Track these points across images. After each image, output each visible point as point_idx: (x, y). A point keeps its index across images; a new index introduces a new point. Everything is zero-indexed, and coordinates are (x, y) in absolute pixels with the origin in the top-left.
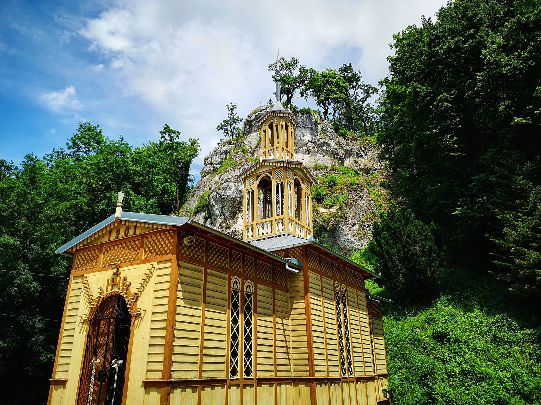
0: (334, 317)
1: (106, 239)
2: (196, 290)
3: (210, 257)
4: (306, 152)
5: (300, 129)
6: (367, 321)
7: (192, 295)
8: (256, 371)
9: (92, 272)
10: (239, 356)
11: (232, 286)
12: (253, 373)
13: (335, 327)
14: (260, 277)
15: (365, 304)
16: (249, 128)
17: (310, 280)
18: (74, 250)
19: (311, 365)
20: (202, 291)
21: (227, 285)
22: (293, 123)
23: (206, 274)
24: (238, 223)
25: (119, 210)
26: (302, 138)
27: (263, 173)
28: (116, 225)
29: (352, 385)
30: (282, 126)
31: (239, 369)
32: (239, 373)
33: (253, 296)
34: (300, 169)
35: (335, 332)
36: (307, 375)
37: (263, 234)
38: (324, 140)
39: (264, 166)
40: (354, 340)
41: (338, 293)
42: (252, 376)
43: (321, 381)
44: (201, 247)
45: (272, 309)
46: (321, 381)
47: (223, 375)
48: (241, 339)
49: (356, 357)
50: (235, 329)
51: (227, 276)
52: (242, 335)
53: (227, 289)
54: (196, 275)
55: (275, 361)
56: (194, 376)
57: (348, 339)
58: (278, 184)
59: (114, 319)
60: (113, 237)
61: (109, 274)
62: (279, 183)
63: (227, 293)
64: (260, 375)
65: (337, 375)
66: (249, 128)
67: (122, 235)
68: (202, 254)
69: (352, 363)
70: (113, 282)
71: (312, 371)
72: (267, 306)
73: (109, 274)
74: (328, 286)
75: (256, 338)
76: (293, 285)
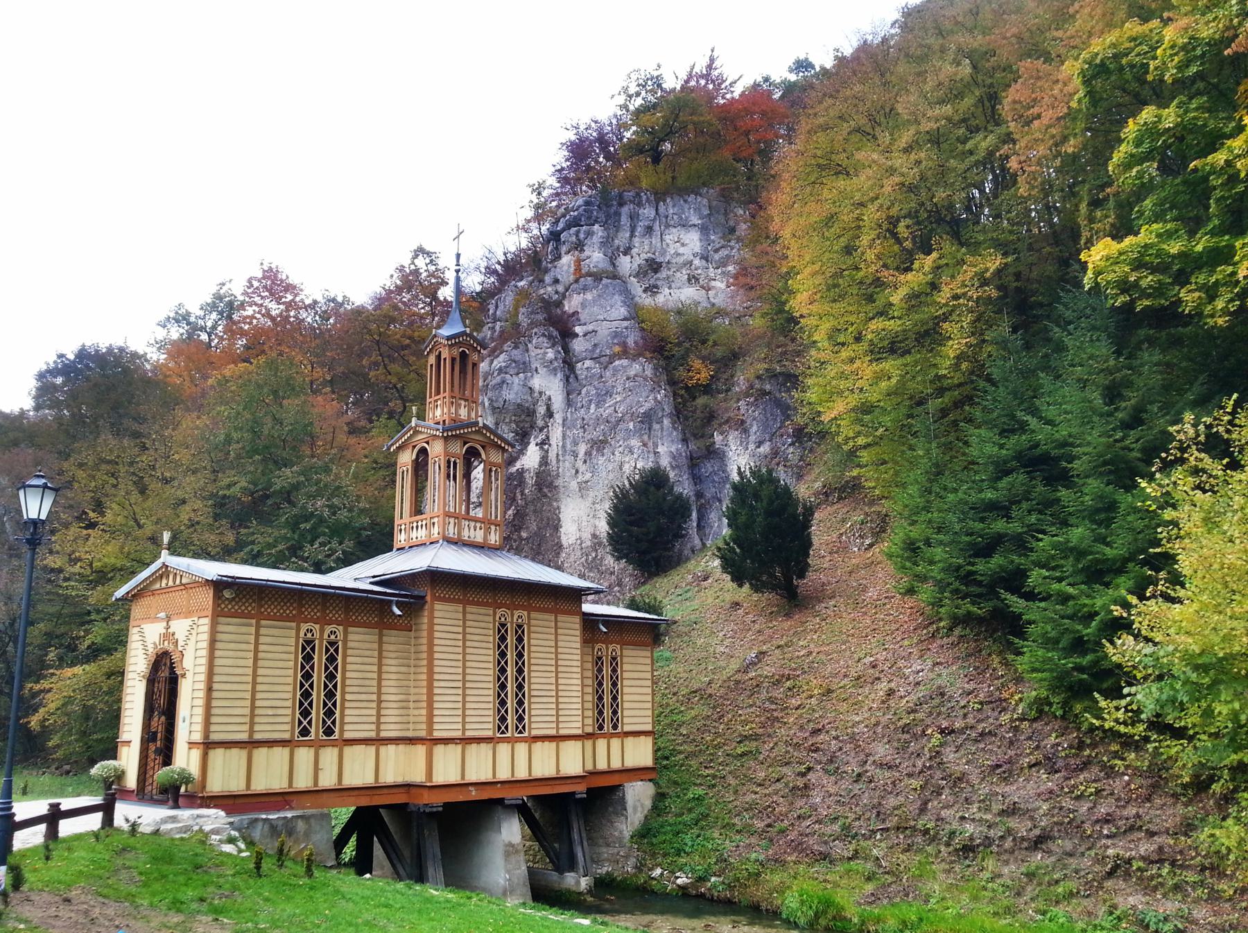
1: (157, 586)
2: (243, 646)
4: (689, 280)
5: (674, 230)
11: (302, 634)
16: (557, 248)
17: (437, 614)
20: (252, 647)
24: (529, 453)
25: (164, 553)
26: (681, 250)
30: (453, 360)
31: (313, 730)
34: (478, 432)
36: (423, 734)
38: (726, 252)
42: (336, 736)
47: (287, 736)
48: (318, 695)
51: (294, 624)
54: (244, 629)
59: (164, 678)
61: (159, 628)
64: (347, 735)
66: (557, 248)
67: (171, 583)
70: (168, 636)
71: (430, 730)
73: (159, 628)
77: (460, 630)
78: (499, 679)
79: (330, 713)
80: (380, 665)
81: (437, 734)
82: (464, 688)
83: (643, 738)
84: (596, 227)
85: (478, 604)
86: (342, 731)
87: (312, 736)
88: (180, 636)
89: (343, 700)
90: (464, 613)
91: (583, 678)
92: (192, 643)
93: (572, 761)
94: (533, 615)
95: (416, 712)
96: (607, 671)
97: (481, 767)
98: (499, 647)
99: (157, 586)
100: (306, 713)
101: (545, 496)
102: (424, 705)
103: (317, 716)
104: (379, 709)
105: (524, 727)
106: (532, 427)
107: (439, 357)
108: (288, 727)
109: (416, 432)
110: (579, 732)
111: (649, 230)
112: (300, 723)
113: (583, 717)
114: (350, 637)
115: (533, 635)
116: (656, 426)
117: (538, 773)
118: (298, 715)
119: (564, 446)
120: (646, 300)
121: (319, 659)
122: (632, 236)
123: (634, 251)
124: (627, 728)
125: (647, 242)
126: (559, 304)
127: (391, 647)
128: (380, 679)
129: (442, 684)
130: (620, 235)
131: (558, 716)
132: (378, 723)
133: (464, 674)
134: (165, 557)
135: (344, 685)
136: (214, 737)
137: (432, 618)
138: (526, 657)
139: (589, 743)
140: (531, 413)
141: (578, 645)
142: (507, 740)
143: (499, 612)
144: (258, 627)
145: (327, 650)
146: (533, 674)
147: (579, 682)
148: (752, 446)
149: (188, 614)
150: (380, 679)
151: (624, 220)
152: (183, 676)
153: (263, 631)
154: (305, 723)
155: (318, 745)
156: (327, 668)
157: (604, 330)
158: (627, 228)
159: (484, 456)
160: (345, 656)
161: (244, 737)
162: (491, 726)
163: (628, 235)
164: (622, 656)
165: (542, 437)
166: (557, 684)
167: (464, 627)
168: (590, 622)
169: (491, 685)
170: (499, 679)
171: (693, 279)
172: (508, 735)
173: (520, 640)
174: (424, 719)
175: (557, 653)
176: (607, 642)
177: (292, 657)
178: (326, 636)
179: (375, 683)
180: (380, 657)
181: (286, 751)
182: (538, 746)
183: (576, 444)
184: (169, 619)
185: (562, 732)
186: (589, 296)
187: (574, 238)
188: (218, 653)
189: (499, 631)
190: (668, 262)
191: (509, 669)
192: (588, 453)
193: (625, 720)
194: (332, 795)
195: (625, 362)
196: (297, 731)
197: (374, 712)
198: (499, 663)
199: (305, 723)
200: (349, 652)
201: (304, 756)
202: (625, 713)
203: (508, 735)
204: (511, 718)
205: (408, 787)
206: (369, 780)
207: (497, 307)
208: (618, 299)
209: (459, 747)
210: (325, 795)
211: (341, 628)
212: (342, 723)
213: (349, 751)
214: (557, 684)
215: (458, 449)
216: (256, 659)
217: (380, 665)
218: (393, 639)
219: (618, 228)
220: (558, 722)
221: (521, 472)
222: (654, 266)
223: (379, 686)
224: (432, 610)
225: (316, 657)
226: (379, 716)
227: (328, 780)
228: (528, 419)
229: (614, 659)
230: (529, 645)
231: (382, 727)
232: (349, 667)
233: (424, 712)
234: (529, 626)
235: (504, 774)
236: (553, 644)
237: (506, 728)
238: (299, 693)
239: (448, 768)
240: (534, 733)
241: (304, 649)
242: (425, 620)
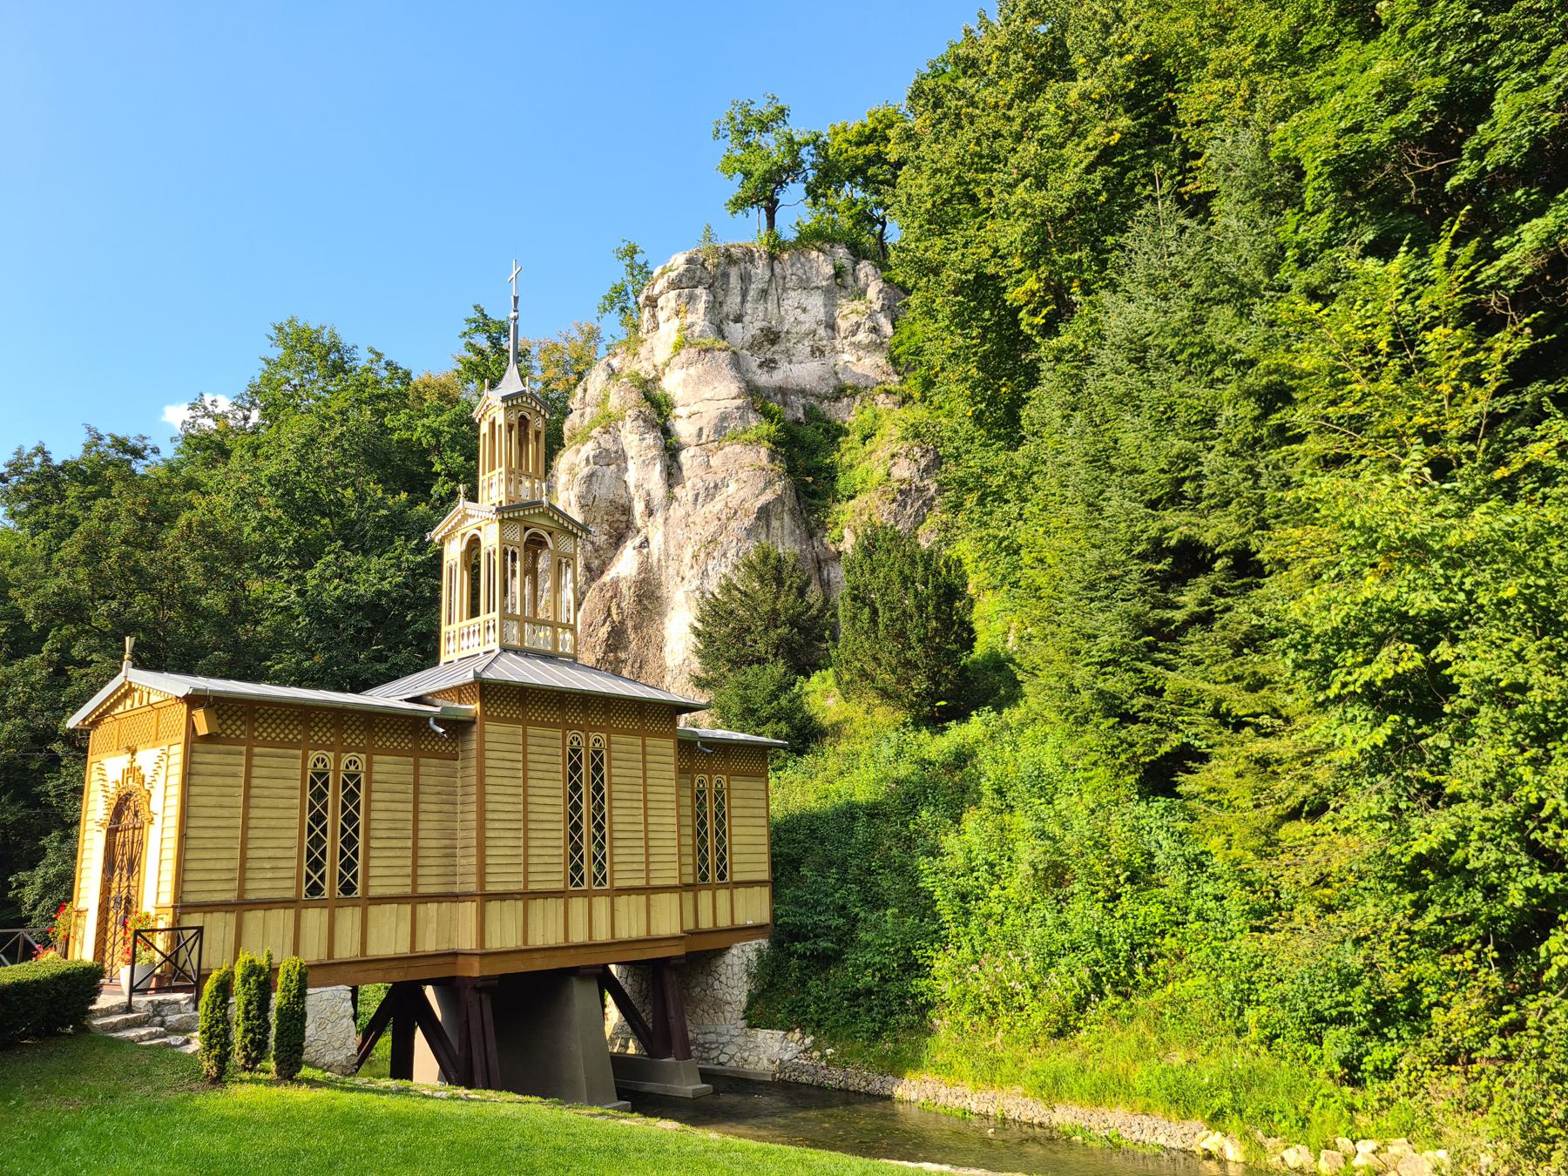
2: (229, 781)
4: (813, 353)
5: (793, 294)
11: (310, 764)
16: (654, 316)
26: (802, 317)
27: (469, 528)
31: (326, 887)
36: (473, 888)
42: (359, 891)
47: (290, 894)
54: (230, 759)
64: (373, 892)
67: (137, 705)
70: (132, 771)
77: (520, 757)
78: (571, 818)
79: (349, 865)
80: (416, 803)
81: (490, 888)
82: (526, 830)
83: (757, 889)
84: (700, 291)
85: (543, 724)
86: (366, 887)
87: (326, 893)
88: (147, 771)
89: (367, 847)
90: (525, 735)
91: (679, 816)
92: (161, 779)
93: (667, 919)
94: (614, 738)
95: (464, 861)
96: (710, 807)
97: (548, 929)
98: (571, 778)
99: (121, 709)
100: (316, 865)
101: (646, 608)
102: (474, 851)
103: (332, 867)
104: (415, 857)
105: (604, 878)
107: (493, 424)
108: (291, 883)
109: (466, 517)
110: (676, 882)
111: (764, 293)
112: (309, 878)
113: (681, 865)
114: (376, 768)
115: (614, 763)
116: (775, 523)
117: (623, 934)
118: (305, 868)
119: (666, 550)
120: (763, 379)
122: (743, 302)
123: (747, 319)
124: (737, 878)
125: (761, 308)
126: (657, 379)
127: (432, 781)
128: (416, 821)
129: (497, 825)
130: (729, 300)
131: (648, 863)
132: (415, 876)
133: (526, 812)
134: (130, 674)
135: (367, 829)
136: (190, 899)
137: (482, 742)
138: (605, 790)
139: (688, 896)
140: (627, 510)
141: (673, 775)
142: (584, 894)
143: (570, 735)
144: (250, 756)
145: (345, 785)
146: (615, 812)
147: (674, 821)
150: (416, 821)
151: (734, 281)
152: (151, 821)
153: (256, 761)
154: (315, 878)
155: (332, 906)
156: (344, 807)
157: (711, 412)
158: (737, 291)
159: (551, 545)
160: (369, 792)
161: (231, 897)
162: (561, 877)
163: (739, 299)
164: (729, 789)
165: (638, 541)
166: (646, 824)
167: (525, 754)
168: (689, 747)
169: (561, 826)
170: (571, 818)
171: (817, 352)
172: (585, 887)
173: (598, 769)
174: (474, 869)
175: (645, 785)
176: (709, 772)
177: (298, 792)
178: (343, 767)
179: (410, 825)
180: (416, 792)
181: (291, 913)
182: (622, 901)
183: (681, 547)
185: (654, 883)
186: (692, 371)
188: (194, 790)
189: (571, 758)
190: (788, 332)
191: (584, 806)
192: (695, 557)
193: (735, 868)
195: (738, 448)
196: (304, 889)
197: (409, 862)
198: (571, 798)
199: (315, 878)
200: (375, 786)
201: (314, 918)
202: (735, 859)
203: (585, 887)
204: (586, 869)
205: (455, 954)
206: (403, 948)
207: (585, 390)
208: (728, 372)
209: (520, 904)
211: (363, 756)
212: (366, 877)
213: (374, 910)
214: (646, 824)
215: (518, 536)
216: (247, 797)
217: (416, 803)
218: (430, 766)
219: (726, 292)
220: (648, 871)
221: (615, 583)
222: (771, 336)
223: (416, 830)
224: (483, 733)
225: (330, 793)
226: (415, 866)
227: (347, 949)
228: (623, 518)
229: (719, 792)
230: (610, 776)
231: (420, 880)
232: (374, 805)
233: (474, 860)
234: (609, 751)
235: (579, 936)
236: (640, 773)
237: (582, 879)
238: (306, 840)
239: (505, 931)
240: (618, 884)
241: (313, 783)
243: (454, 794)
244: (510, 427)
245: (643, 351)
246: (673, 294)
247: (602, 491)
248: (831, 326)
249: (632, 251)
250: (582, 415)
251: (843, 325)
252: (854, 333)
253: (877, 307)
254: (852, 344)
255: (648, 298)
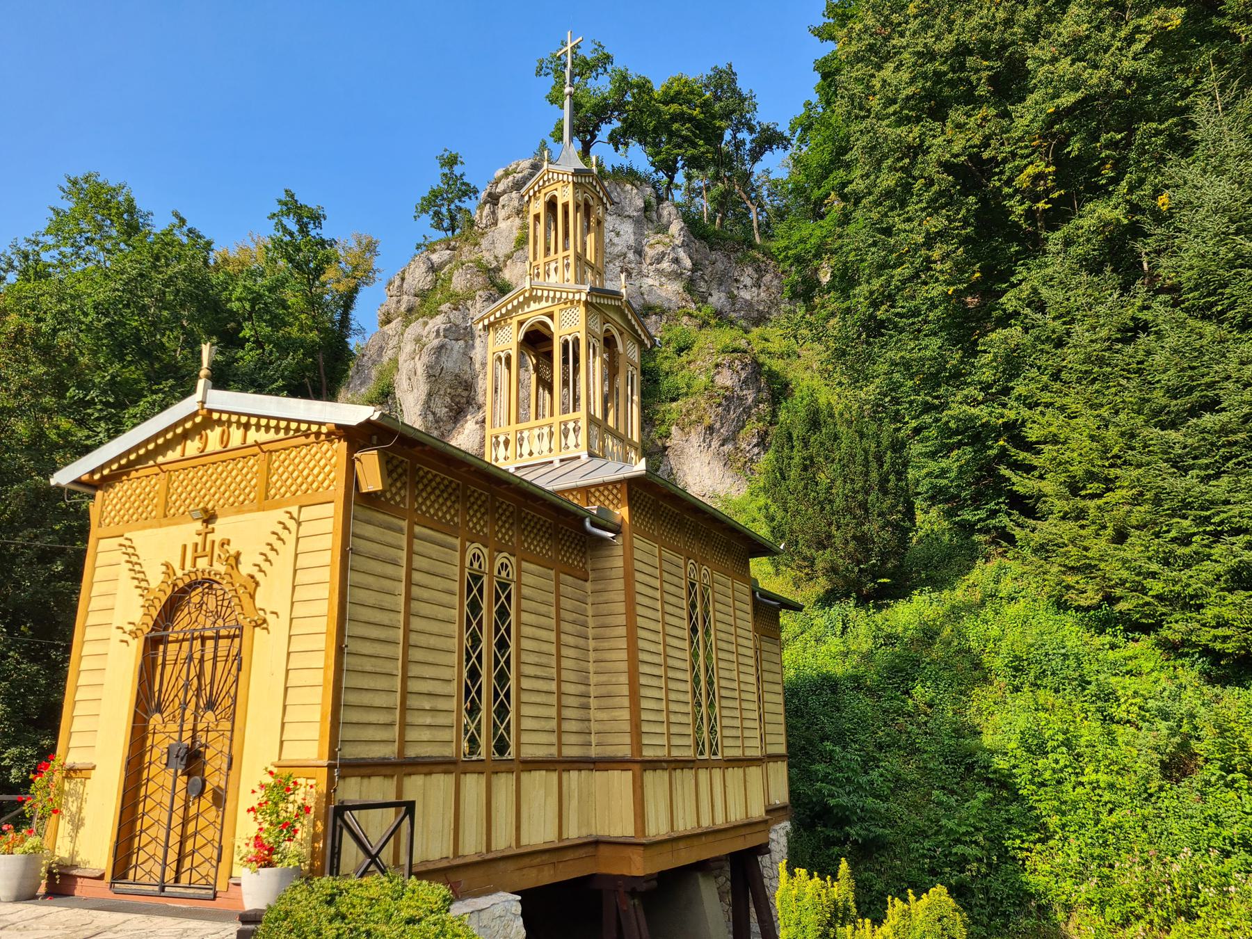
0: (686, 634)
3: (420, 500)
6: (750, 644)
7: (382, 580)
8: (518, 744)
9: (144, 528)
10: (483, 714)
12: (512, 749)
13: (687, 655)
14: (529, 547)
15: (749, 608)
16: (493, 213)
17: (637, 554)
18: (97, 477)
19: (637, 732)
20: (403, 573)
21: (458, 562)
22: (601, 199)
23: (412, 536)
24: (466, 432)
26: (616, 240)
27: (533, 313)
28: (198, 420)
29: (717, 773)
32: (483, 750)
33: (513, 586)
34: (618, 310)
35: (687, 665)
36: (625, 751)
37: (531, 454)
39: (538, 299)
40: (723, 683)
41: (693, 585)
42: (512, 752)
43: (654, 764)
44: (400, 475)
45: (553, 615)
46: (654, 764)
47: (449, 752)
49: (727, 718)
50: (474, 656)
51: (457, 542)
52: (489, 668)
53: (457, 570)
55: (559, 725)
56: (389, 752)
57: (710, 683)
58: (566, 342)
60: (192, 447)
62: (570, 338)
63: (457, 578)
64: (527, 752)
65: (689, 753)
68: (402, 492)
69: (718, 729)
71: (637, 744)
72: (543, 609)
74: (673, 569)
75: (519, 676)
76: (599, 566)
106: (469, 403)
121: (487, 612)
126: (498, 269)
140: (469, 386)
148: (715, 444)
149: (266, 500)
155: (489, 770)
159: (620, 348)
172: (706, 757)
174: (627, 727)
178: (496, 573)
181: (451, 779)
184: (209, 518)
187: (516, 203)
194: (511, 866)
199: (472, 728)
205: (596, 843)
210: (502, 865)
212: (519, 731)
228: (465, 394)
242: (619, 562)
243: (585, 625)
244: (577, 207)
245: (484, 243)
246: (514, 194)
247: (450, 364)
248: (639, 252)
249: (452, 161)
250: (399, 302)
251: (650, 253)
252: (659, 261)
253: (678, 242)
254: (657, 270)
255: (490, 195)
